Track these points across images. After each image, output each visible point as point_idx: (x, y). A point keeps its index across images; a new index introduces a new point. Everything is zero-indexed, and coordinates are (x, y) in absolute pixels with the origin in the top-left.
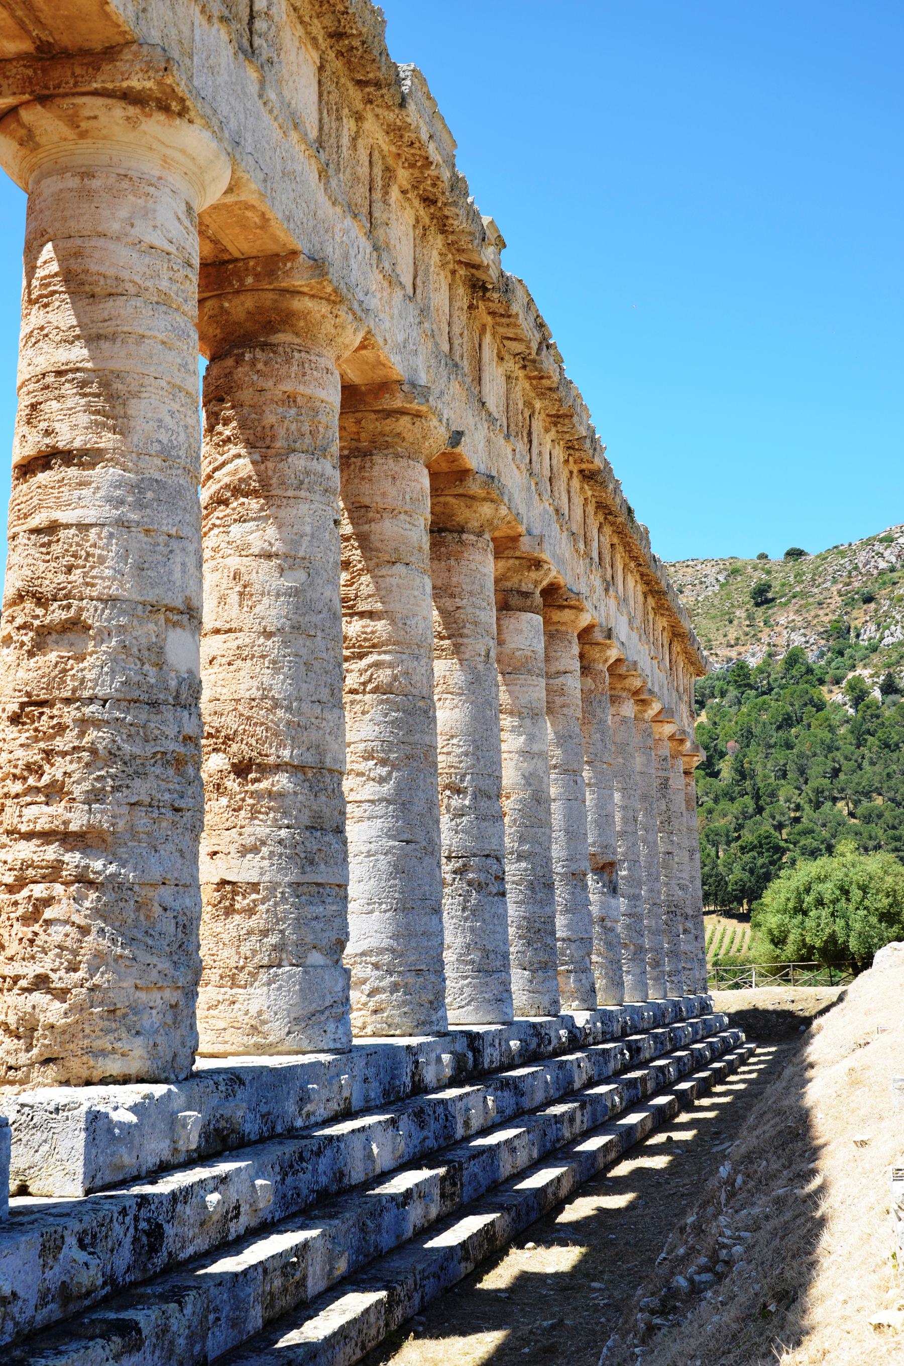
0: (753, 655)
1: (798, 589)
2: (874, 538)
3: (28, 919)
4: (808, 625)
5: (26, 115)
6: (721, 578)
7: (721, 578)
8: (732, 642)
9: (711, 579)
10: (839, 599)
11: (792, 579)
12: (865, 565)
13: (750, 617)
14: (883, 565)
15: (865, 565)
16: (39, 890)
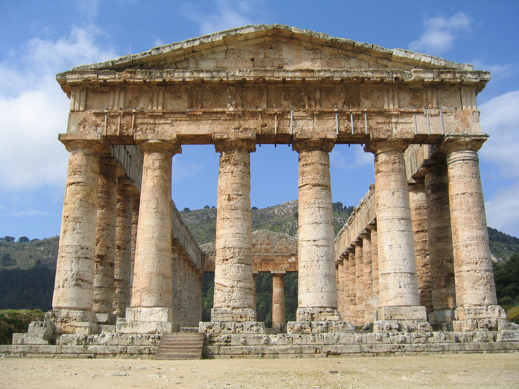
14: (283, 214)
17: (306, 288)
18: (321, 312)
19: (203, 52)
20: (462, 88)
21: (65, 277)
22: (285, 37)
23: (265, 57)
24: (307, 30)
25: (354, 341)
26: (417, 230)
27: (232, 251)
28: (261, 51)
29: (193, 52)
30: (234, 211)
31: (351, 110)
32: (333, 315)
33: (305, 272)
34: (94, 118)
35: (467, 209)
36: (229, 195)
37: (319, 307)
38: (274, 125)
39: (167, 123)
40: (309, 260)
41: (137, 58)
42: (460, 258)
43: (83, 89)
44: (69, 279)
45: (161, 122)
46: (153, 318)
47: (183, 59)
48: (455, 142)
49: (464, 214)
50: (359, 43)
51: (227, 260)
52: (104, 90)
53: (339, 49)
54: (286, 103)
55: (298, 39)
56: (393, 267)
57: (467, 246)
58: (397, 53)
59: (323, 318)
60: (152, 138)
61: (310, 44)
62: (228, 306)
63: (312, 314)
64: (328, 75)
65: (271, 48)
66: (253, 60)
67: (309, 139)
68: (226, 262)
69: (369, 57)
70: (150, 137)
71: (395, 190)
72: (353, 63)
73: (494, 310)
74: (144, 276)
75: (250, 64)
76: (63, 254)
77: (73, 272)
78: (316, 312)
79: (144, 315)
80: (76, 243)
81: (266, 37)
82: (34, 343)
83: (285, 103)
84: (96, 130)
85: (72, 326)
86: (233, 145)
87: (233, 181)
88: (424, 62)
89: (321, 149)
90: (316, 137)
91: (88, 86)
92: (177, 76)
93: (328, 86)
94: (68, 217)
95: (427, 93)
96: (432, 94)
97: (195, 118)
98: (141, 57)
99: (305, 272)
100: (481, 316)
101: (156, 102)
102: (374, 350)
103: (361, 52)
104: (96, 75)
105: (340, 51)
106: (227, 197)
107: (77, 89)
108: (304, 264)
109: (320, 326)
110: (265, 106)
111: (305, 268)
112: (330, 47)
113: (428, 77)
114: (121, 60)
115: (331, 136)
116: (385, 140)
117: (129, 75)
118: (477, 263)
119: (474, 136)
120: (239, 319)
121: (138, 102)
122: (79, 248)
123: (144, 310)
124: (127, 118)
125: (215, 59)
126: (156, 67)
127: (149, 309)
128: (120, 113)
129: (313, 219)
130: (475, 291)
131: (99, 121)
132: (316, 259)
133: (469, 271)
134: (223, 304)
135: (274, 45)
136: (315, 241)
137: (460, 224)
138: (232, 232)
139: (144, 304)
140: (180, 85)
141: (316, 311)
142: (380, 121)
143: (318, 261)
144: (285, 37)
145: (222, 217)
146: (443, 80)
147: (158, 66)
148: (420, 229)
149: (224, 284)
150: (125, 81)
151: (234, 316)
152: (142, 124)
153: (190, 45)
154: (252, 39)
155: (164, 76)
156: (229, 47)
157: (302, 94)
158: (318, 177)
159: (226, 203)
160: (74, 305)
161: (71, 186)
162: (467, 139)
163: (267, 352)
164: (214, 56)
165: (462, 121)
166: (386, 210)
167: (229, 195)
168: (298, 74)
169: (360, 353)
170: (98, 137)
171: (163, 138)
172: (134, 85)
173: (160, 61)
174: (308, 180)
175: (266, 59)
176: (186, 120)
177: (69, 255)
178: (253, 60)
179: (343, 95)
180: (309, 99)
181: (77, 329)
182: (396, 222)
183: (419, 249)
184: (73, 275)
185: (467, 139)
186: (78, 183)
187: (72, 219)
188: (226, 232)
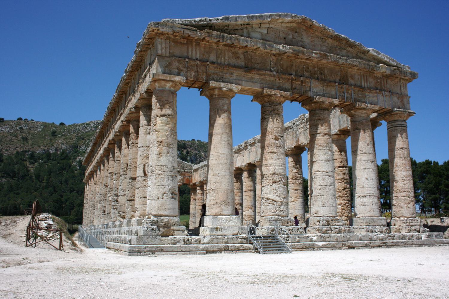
0: (51, 149)
1: (63, 134)
2: (85, 123)
3: (347, 207)
4: (67, 143)
5: (341, 135)
6: (42, 127)
7: (42, 127)
8: (46, 145)
9: (39, 127)
10: (75, 138)
11: (62, 130)
12: (82, 130)
13: (51, 139)
14: (87, 131)
15: (82, 130)
16: (348, 205)
17: (322, 204)
18: (332, 220)
19: (253, 26)
20: (401, 80)
21: (163, 191)
22: (305, 26)
23: (293, 38)
24: (323, 25)
25: (358, 239)
26: (339, 165)
27: (280, 176)
28: (290, 33)
29: (248, 24)
30: (279, 148)
31: (345, 85)
32: (339, 222)
33: (322, 193)
35: (404, 158)
36: (276, 136)
37: (331, 217)
39: (231, 76)
40: (324, 184)
41: (212, 22)
42: (399, 188)
44: (167, 192)
45: (227, 75)
46: (231, 223)
47: (240, 28)
48: (398, 115)
49: (402, 161)
50: (351, 40)
51: (276, 182)
52: (183, 42)
53: (337, 41)
54: (307, 74)
55: (313, 29)
56: (368, 192)
57: (403, 181)
58: (372, 51)
59: (334, 224)
60: (224, 87)
61: (320, 35)
62: (279, 215)
63: (328, 222)
65: (296, 32)
66: (285, 38)
67: (323, 102)
68: (275, 184)
69: (353, 50)
71: (369, 142)
73: (418, 220)
74: (223, 192)
76: (160, 172)
77: (170, 187)
78: (331, 220)
79: (225, 221)
80: (170, 164)
81: (294, 23)
82: (154, 243)
83: (307, 74)
85: (173, 230)
86: (277, 99)
87: (277, 126)
88: (386, 61)
91: (172, 37)
93: (331, 66)
94: (161, 142)
95: (384, 81)
96: (387, 82)
97: (250, 75)
98: (215, 21)
99: (322, 193)
100: (412, 224)
101: (223, 59)
102: (372, 245)
103: (349, 47)
104: (182, 30)
105: (337, 43)
106: (274, 137)
107: (162, 37)
108: (320, 187)
109: (336, 229)
110: (294, 73)
111: (321, 190)
112: (332, 38)
114: (201, 21)
118: (409, 192)
120: (287, 225)
121: (209, 56)
122: (173, 168)
123: (224, 217)
125: (261, 33)
126: (221, 31)
127: (228, 217)
128: (197, 63)
129: (325, 157)
130: (408, 209)
131: (181, 67)
132: (329, 184)
133: (404, 196)
134: (275, 213)
135: (298, 30)
136: (327, 172)
137: (399, 166)
138: (279, 163)
139: (224, 212)
140: (240, 48)
141: (330, 219)
142: (360, 95)
143: (330, 186)
144: (305, 26)
145: (271, 151)
147: (222, 30)
148: (342, 165)
149: (275, 199)
150: (204, 38)
151: (283, 222)
154: (285, 23)
155: (233, 40)
156: (271, 26)
157: (316, 69)
158: (328, 129)
159: (273, 141)
160: (172, 214)
161: (162, 117)
163: (316, 246)
164: (259, 30)
165: (401, 102)
166: (363, 154)
167: (276, 136)
169: (365, 246)
170: (184, 79)
171: (231, 88)
172: (206, 42)
173: (224, 27)
174: (321, 130)
175: (294, 40)
176: (244, 77)
177: (166, 173)
178: (285, 38)
179: (339, 74)
181: (176, 232)
182: (369, 163)
183: (341, 178)
184: (170, 189)
186: (169, 115)
187: (166, 144)
188: (275, 162)
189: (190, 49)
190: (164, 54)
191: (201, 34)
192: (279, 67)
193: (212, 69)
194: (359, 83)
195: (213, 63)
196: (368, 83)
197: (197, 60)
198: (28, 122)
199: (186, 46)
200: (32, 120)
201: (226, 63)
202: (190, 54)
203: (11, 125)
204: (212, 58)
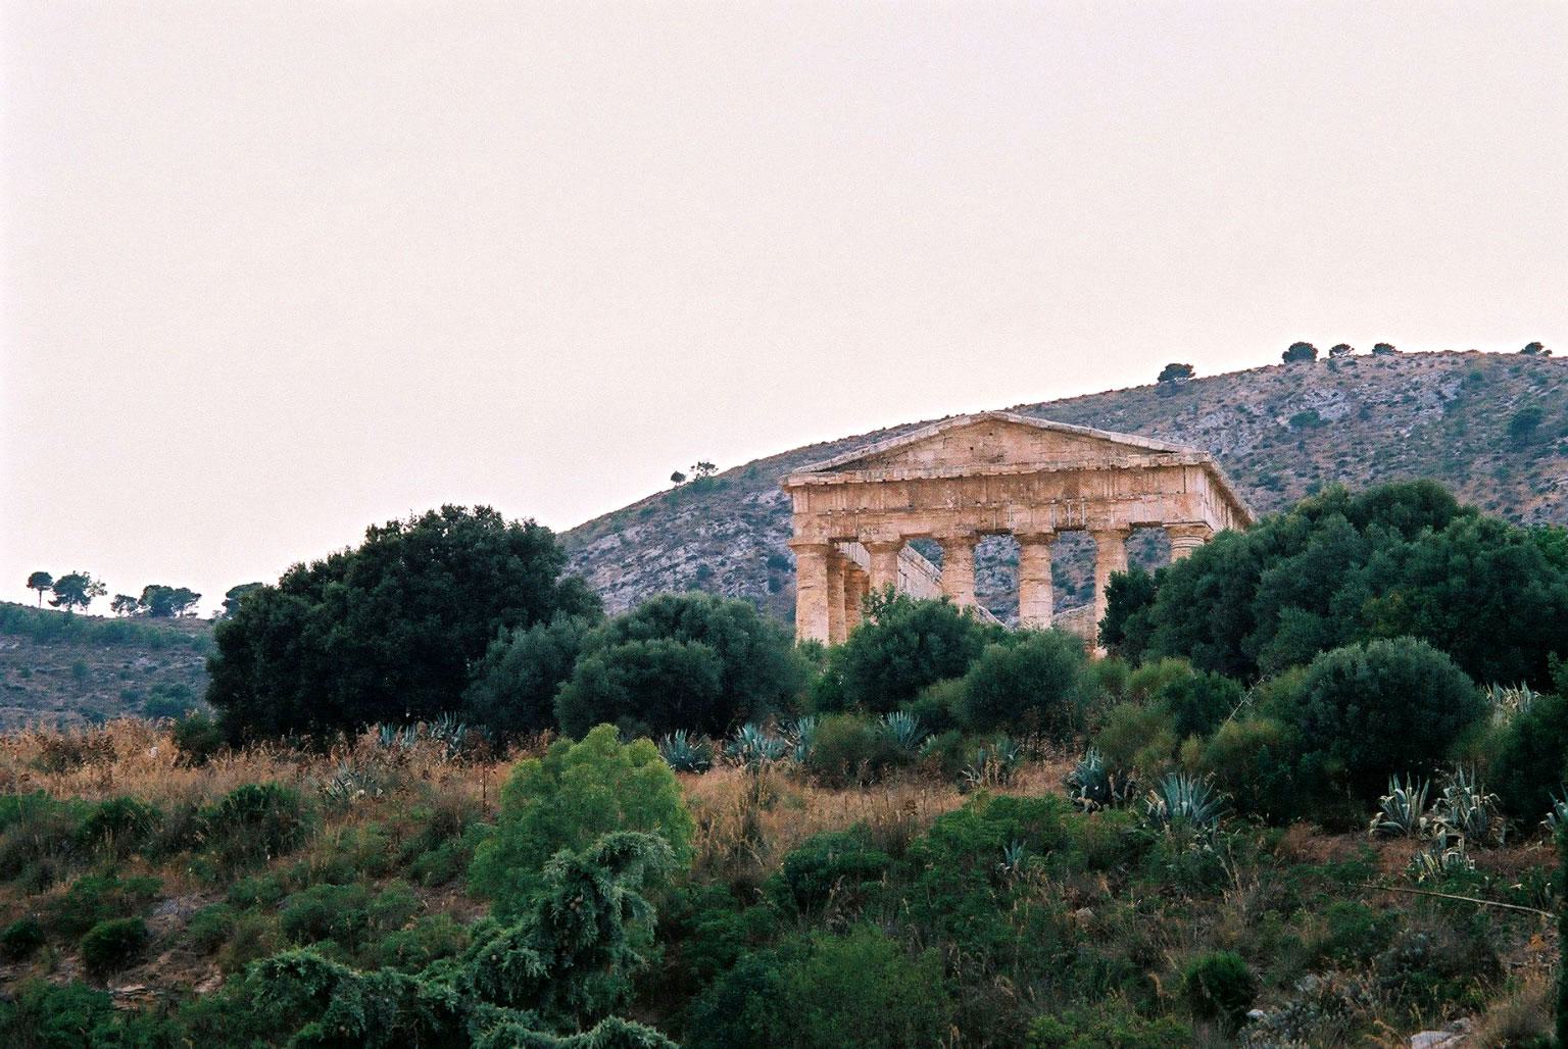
6: (1449, 391)
7: (1449, 391)
34: (817, 520)
38: (992, 520)
43: (804, 491)
64: (1043, 466)
65: (991, 434)
66: (972, 449)
70: (874, 537)
72: (1075, 446)
75: (968, 454)
83: (1004, 496)
84: (821, 533)
89: (1040, 543)
90: (1032, 533)
92: (896, 476)
97: (916, 515)
110: (984, 500)
113: (1145, 461)
115: (1048, 529)
116: (1101, 531)
117: (849, 476)
119: (1191, 523)
124: (851, 519)
146: (1160, 465)
150: (846, 482)
152: (866, 524)
153: (906, 442)
162: (1184, 526)
168: (1014, 467)
180: (1028, 490)
185: (1184, 526)
189: (834, 498)
190: (802, 511)
191: (838, 478)
192: (960, 496)
193: (863, 519)
194: (1098, 492)
195: (864, 511)
196: (1116, 489)
197: (844, 510)
198: (1350, 370)
199: (829, 495)
200: (1381, 348)
201: (882, 507)
202: (834, 504)
203: (1240, 409)
204: (864, 503)
